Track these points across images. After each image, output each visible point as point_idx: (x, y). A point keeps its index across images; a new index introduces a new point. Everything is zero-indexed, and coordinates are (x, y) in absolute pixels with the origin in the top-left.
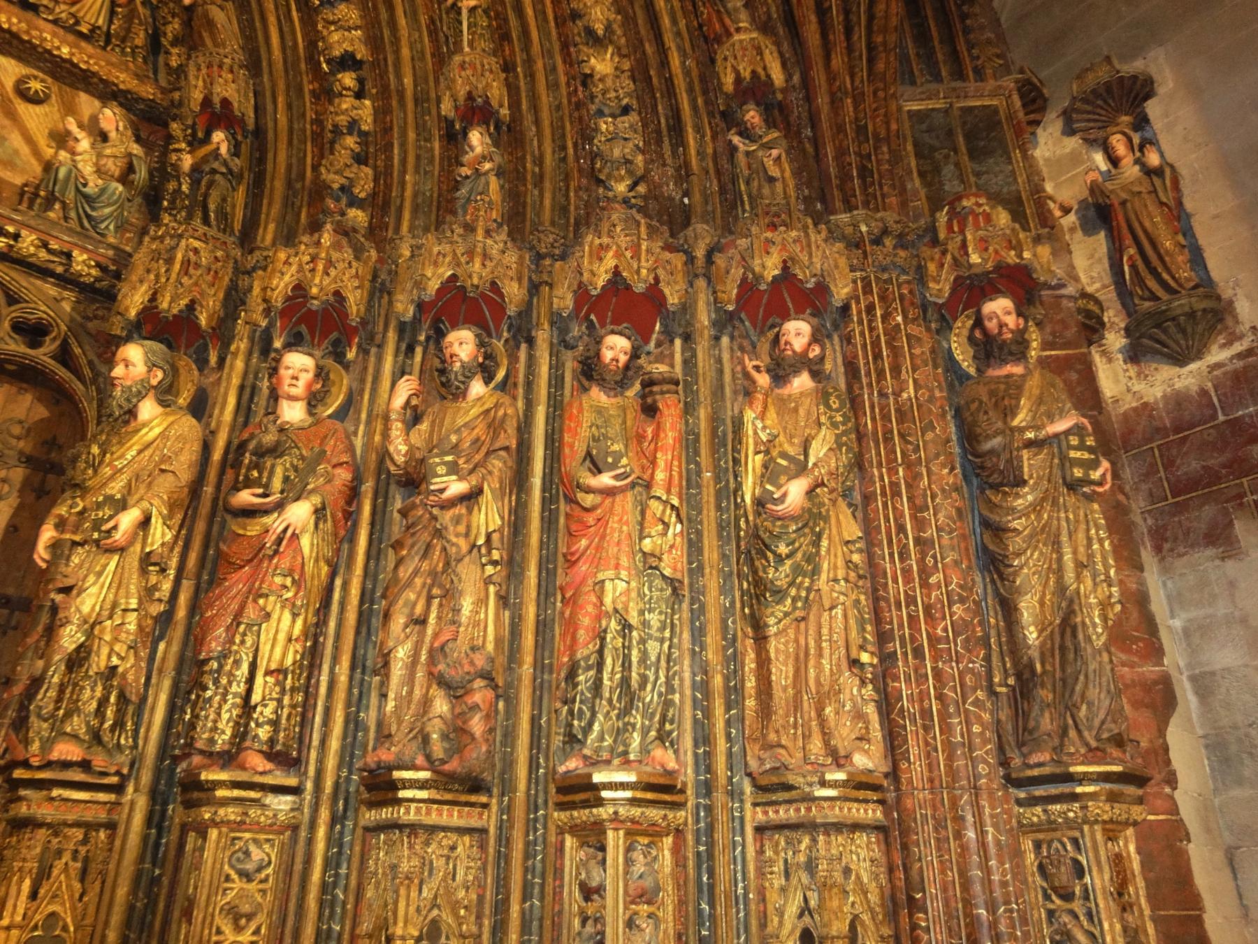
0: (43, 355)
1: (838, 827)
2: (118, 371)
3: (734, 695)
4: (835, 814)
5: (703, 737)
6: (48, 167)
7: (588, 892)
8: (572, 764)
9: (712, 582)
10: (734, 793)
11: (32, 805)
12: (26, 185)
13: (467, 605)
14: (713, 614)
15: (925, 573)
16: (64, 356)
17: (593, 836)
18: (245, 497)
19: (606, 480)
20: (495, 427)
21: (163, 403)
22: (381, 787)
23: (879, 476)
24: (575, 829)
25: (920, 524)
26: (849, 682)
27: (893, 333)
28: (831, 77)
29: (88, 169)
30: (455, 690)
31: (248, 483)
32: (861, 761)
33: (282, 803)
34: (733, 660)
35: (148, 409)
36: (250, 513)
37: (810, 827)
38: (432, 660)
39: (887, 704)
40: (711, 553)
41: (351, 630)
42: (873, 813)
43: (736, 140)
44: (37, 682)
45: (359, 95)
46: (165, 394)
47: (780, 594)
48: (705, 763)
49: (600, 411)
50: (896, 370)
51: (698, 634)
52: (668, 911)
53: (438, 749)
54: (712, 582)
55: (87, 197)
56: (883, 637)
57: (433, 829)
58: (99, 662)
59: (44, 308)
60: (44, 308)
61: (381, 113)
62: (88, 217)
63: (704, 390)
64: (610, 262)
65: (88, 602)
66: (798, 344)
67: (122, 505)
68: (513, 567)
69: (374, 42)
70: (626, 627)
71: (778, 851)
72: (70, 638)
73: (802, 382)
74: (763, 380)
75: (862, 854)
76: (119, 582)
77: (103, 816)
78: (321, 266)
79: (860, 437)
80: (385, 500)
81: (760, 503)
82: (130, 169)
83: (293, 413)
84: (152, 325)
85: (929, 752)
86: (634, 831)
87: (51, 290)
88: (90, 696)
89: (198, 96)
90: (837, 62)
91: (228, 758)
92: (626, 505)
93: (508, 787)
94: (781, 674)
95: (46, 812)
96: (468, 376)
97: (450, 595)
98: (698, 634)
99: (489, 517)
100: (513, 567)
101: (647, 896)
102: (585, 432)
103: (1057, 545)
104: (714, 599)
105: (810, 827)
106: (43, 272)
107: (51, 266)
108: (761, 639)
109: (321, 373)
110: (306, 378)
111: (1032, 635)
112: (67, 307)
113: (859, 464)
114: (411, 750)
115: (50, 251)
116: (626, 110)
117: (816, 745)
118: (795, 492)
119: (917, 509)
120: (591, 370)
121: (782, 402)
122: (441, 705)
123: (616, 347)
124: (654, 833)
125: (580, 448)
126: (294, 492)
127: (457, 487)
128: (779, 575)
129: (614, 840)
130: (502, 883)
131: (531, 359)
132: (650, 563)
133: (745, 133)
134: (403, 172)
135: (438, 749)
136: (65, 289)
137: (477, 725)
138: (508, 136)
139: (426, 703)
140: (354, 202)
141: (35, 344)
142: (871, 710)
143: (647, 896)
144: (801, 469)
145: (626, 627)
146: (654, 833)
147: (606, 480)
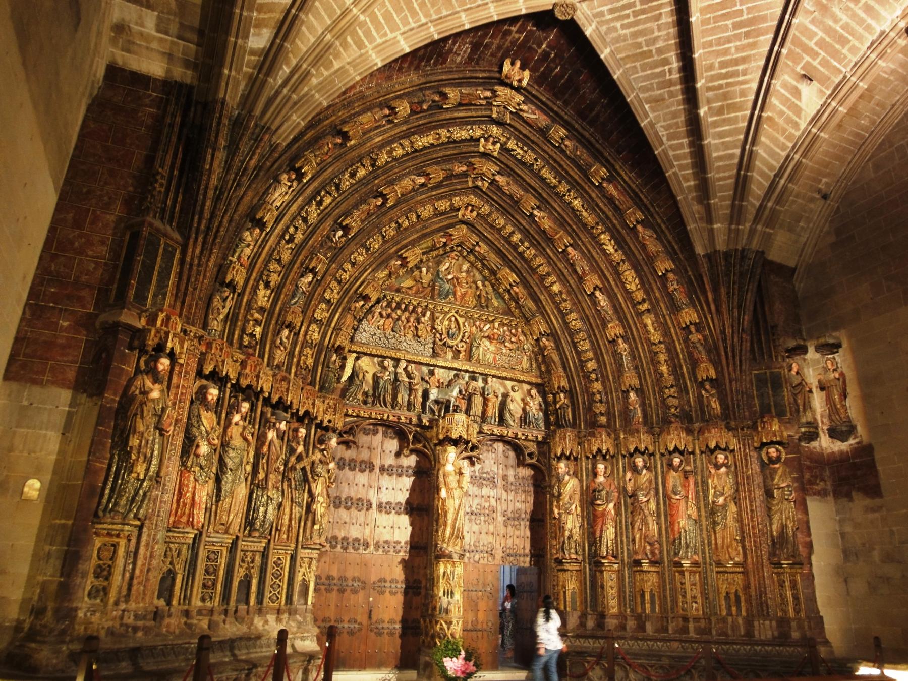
0: (534, 461)
1: (733, 572)
2: (560, 470)
3: (709, 544)
4: (731, 570)
5: (704, 552)
7: (682, 584)
8: (677, 559)
9: (704, 519)
10: (711, 565)
11: (567, 567)
13: (651, 526)
14: (704, 527)
15: (752, 517)
17: (682, 573)
18: (599, 502)
19: (678, 497)
20: (650, 482)
21: (569, 475)
22: (638, 563)
23: (742, 495)
24: (678, 571)
25: (751, 506)
26: (735, 544)
27: (746, 455)
28: (729, 374)
30: (651, 544)
31: (599, 499)
32: (737, 559)
33: (616, 566)
34: (709, 537)
35: (567, 477)
36: (599, 505)
37: (727, 572)
38: (645, 538)
39: (744, 547)
40: (703, 513)
41: (625, 529)
42: (741, 569)
43: (703, 392)
44: (564, 542)
45: (597, 380)
46: (568, 473)
47: (719, 524)
48: (704, 558)
49: (674, 477)
50: (746, 466)
51: (701, 530)
52: (698, 588)
53: (650, 556)
54: (704, 519)
56: (743, 532)
57: (649, 572)
58: (575, 537)
61: (603, 383)
63: (699, 472)
64: (674, 444)
65: (569, 526)
66: (721, 461)
67: (571, 505)
68: (659, 516)
69: (598, 361)
70: (685, 531)
71: (721, 576)
72: (567, 533)
73: (723, 469)
74: (713, 471)
75: (739, 578)
76: (573, 521)
77: (577, 568)
78: (604, 442)
79: (737, 483)
80: (629, 501)
81: (714, 502)
82: (540, 405)
83: (601, 479)
84: (563, 456)
85: (752, 557)
86: (690, 572)
88: (573, 545)
89: (556, 387)
90: (731, 369)
91: (604, 558)
92: (683, 503)
93: (663, 562)
94: (720, 541)
95: (570, 568)
96: (642, 470)
97: (647, 524)
98: (701, 530)
99: (652, 506)
100: (659, 516)
101: (694, 584)
102: (671, 484)
103: (781, 513)
104: (704, 523)
105: (727, 572)
108: (715, 533)
109: (606, 468)
110: (603, 470)
111: (775, 533)
113: (737, 491)
114: (644, 557)
116: (672, 386)
117: (727, 556)
118: (721, 500)
119: (751, 502)
120: (670, 465)
121: (718, 475)
122: (648, 548)
123: (677, 461)
124: (695, 572)
125: (671, 488)
126: (608, 502)
127: (645, 500)
128: (718, 519)
129: (687, 574)
130: (664, 581)
131: (655, 460)
132: (689, 516)
133: (706, 390)
134: (614, 407)
135: (650, 556)
137: (657, 552)
138: (640, 392)
139: (645, 547)
140: (602, 414)
142: (740, 548)
143: (694, 584)
144: (723, 494)
145: (685, 531)
146: (695, 572)
147: (678, 497)
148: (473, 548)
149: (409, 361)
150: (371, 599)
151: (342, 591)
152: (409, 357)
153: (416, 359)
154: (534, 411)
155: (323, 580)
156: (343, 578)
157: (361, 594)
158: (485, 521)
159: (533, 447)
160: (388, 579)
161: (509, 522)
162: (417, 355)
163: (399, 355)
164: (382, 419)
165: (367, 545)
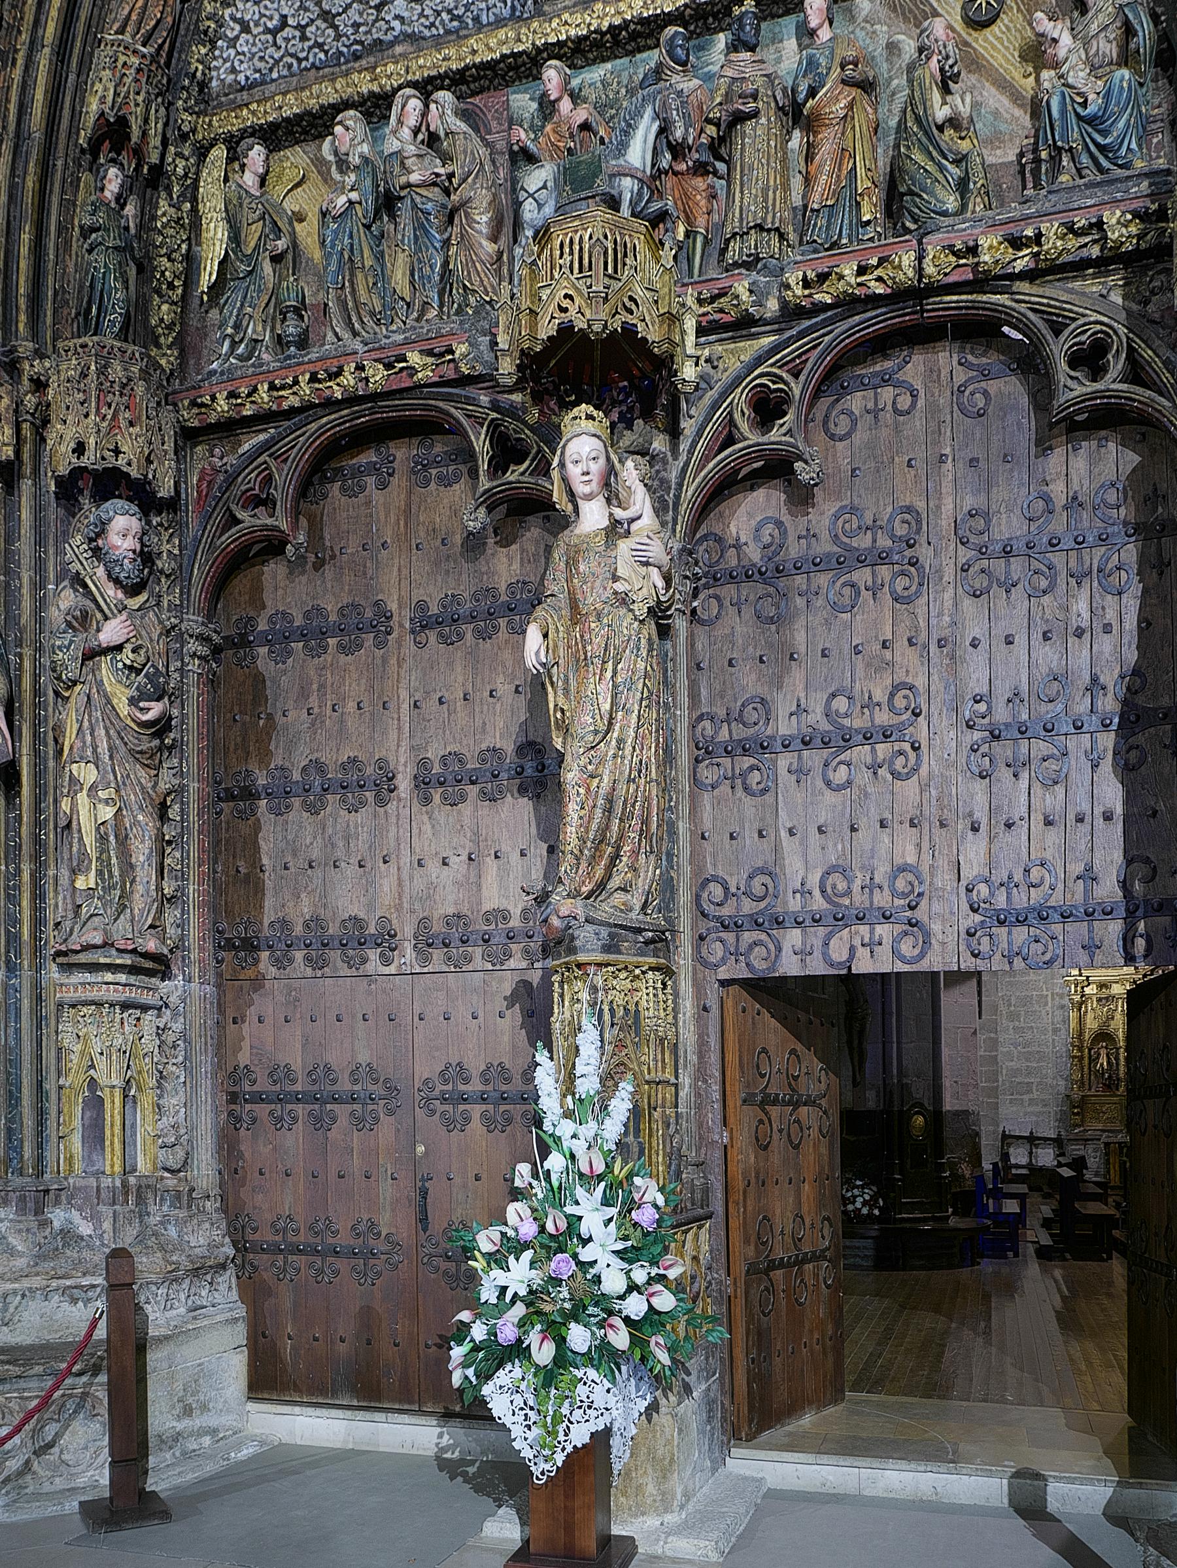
0: (1112, 382)
6: (1037, 108)
12: (1021, 155)
16: (1136, 373)
29: (1079, 77)
55: (1091, 121)
59: (1095, 317)
60: (1095, 317)
62: (1102, 149)
87: (1092, 286)
106: (1078, 267)
107: (1084, 253)
112: (1117, 298)
115: (1078, 234)
136: (1108, 273)
141: (1097, 373)
148: (819, 903)
149: (426, 88)
150: (421, 1149)
151: (320, 1123)
152: (428, 63)
153: (453, 58)
154: (1079, 77)
155: (263, 1084)
156: (322, 1072)
157: (386, 1130)
158: (874, 768)
159: (1098, 303)
160: (475, 1066)
161: (1004, 750)
162: (456, 35)
163: (391, 73)
164: (352, 400)
165: (387, 941)
